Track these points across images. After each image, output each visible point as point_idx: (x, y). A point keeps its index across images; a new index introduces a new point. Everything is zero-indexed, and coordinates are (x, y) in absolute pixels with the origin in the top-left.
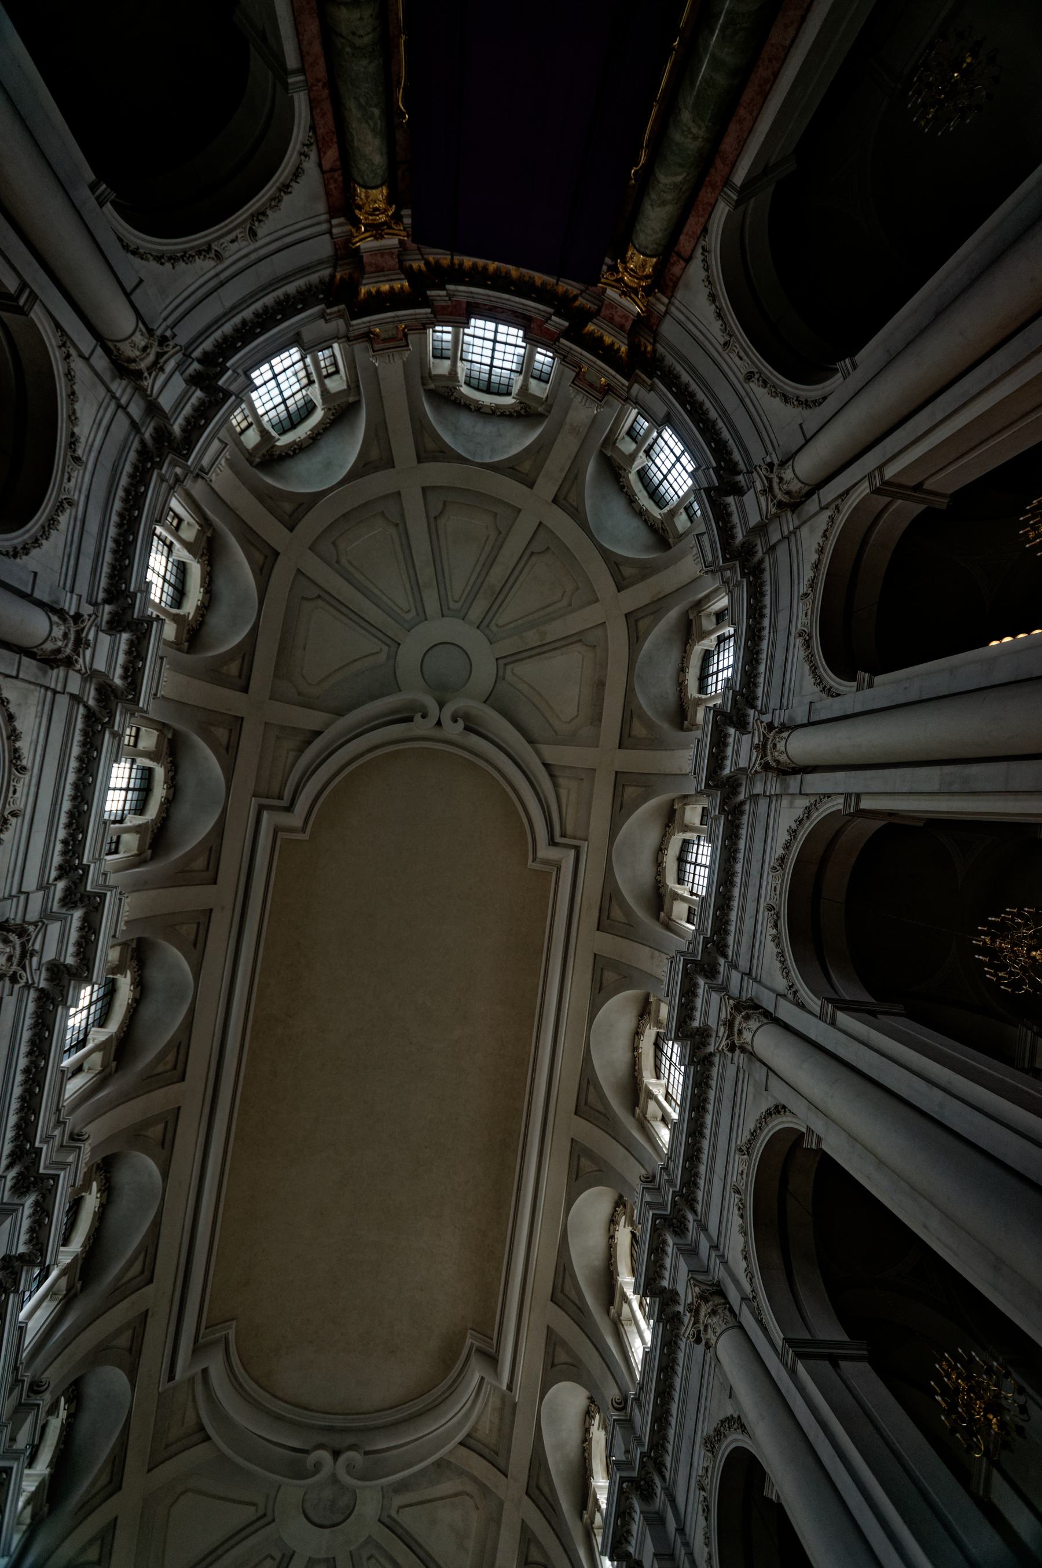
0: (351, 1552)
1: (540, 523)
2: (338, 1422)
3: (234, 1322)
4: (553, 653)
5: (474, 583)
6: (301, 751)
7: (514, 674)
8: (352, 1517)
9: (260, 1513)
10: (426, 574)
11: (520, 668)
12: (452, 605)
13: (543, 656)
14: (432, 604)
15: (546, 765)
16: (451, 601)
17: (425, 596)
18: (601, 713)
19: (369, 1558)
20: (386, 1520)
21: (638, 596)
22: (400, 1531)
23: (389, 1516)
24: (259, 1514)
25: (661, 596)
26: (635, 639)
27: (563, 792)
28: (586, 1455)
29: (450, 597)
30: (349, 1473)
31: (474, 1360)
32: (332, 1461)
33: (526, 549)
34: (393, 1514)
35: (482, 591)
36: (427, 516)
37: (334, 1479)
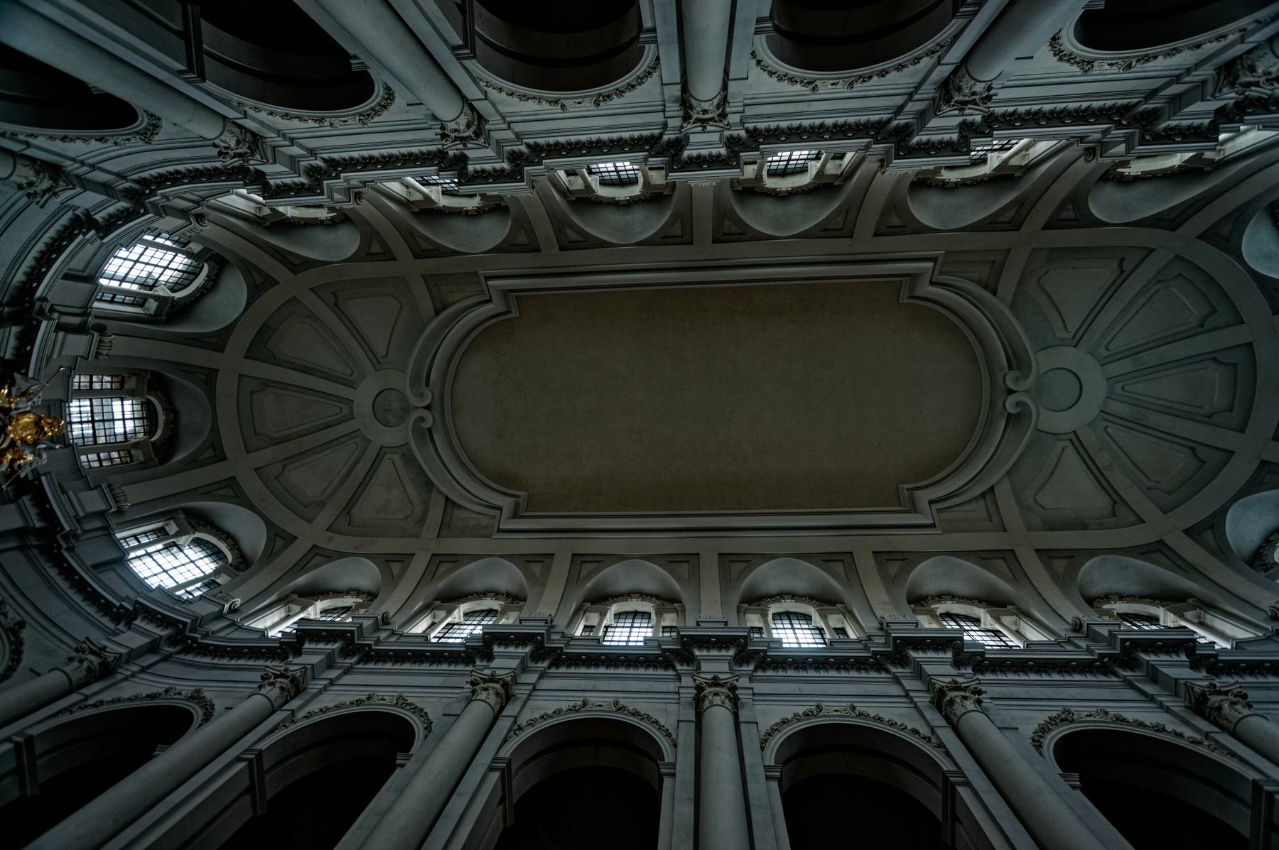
0: (359, 430)
1: (1233, 453)
2: (447, 406)
3: (518, 315)
4: (1094, 481)
5: (1148, 402)
6: (979, 283)
7: (1063, 449)
9: (381, 360)
10: (1148, 358)
11: (1070, 453)
12: (1118, 387)
13: (1088, 472)
14: (1115, 369)
15: (992, 489)
16: (1122, 384)
17: (1126, 360)
18: (1057, 530)
19: (356, 443)
21: (1191, 551)
22: (377, 463)
23: (385, 453)
24: (379, 359)
25: (1203, 571)
26: (1142, 552)
27: (973, 506)
28: (470, 597)
29: (1126, 382)
30: (416, 420)
31: (511, 500)
32: (423, 405)
33: (1196, 442)
34: (387, 456)
35: (1141, 409)
36: (1215, 351)
37: (407, 409)
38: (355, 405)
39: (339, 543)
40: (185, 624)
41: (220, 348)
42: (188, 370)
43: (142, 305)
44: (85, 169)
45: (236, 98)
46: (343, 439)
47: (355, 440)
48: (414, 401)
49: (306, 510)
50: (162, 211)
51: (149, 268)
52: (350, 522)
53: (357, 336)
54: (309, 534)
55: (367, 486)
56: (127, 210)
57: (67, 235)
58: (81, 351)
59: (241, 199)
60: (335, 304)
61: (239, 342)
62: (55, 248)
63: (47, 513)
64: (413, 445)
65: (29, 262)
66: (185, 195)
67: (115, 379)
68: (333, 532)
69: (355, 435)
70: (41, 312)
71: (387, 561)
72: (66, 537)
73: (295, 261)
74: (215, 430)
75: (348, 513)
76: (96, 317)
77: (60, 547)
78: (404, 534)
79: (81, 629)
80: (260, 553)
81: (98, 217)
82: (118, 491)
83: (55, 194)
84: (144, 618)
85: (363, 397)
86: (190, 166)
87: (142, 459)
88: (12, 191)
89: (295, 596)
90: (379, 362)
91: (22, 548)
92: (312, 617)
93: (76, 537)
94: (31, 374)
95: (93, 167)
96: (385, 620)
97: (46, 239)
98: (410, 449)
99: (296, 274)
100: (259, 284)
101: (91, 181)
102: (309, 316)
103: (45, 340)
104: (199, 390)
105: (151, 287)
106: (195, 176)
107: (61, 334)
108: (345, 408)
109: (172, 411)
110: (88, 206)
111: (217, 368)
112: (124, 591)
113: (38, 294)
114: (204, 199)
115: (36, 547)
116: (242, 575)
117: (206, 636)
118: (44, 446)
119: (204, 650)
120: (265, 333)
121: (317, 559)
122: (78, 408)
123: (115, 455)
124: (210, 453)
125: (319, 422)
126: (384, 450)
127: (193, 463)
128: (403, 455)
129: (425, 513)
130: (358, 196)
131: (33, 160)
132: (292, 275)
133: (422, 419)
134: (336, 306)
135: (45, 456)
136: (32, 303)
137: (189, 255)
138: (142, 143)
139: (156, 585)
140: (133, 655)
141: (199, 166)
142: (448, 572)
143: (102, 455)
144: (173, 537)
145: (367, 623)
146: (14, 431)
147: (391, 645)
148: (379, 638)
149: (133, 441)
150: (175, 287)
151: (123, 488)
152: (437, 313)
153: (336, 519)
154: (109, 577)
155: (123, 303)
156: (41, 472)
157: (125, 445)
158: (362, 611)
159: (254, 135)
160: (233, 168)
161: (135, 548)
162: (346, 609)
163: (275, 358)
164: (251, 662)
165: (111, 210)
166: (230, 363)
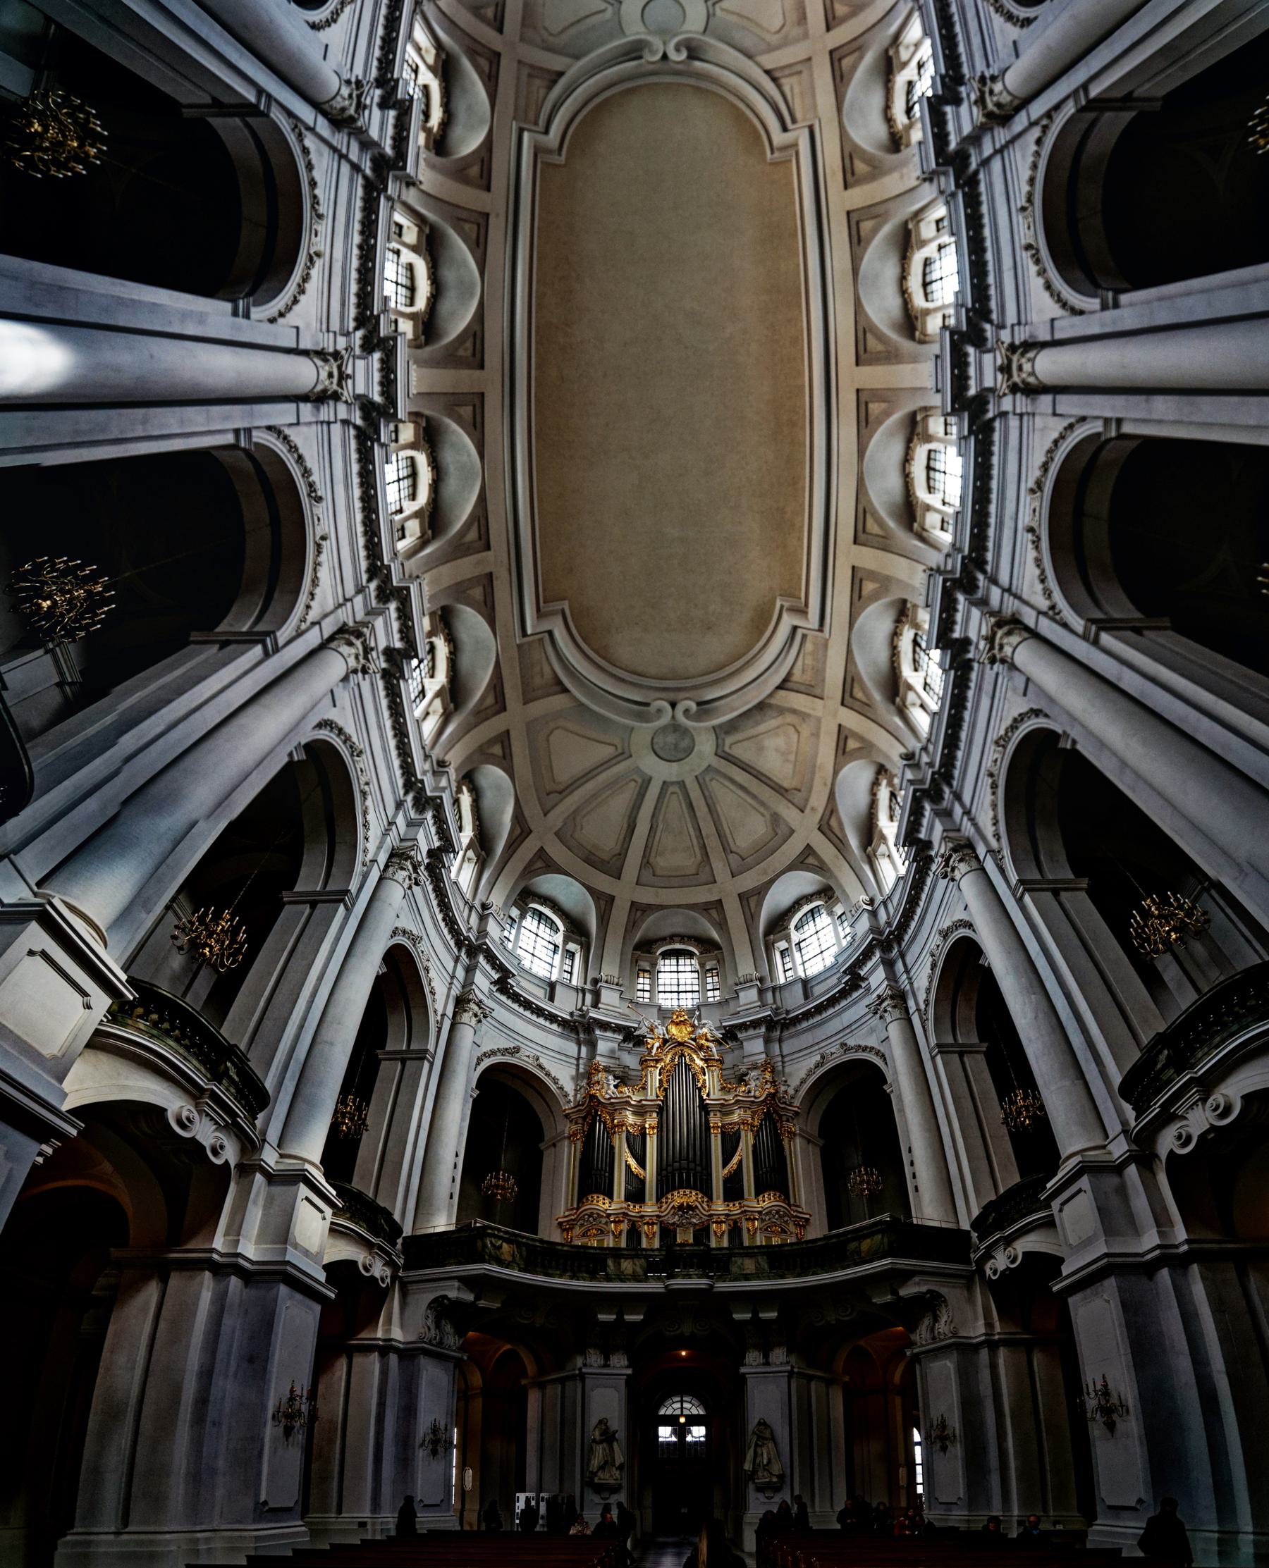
8: (693, 754)
9: (620, 751)
20: (723, 754)
22: (733, 760)
23: (724, 751)
34: (727, 749)
37: (675, 727)
38: (668, 780)
39: (818, 801)
40: (873, 939)
41: (611, 899)
42: (632, 925)
43: (572, 955)
44: (455, 981)
45: (358, 868)
46: (707, 794)
47: (707, 779)
48: (666, 719)
49: (779, 832)
50: (483, 933)
51: (538, 946)
52: (796, 789)
53: (595, 772)
54: (805, 830)
55: (759, 772)
56: (486, 957)
57: (516, 997)
58: (617, 995)
59: (461, 872)
60: (560, 793)
61: (604, 883)
62: (527, 1005)
63: (755, 1024)
64: (716, 722)
65: (541, 1021)
66: (466, 918)
67: (641, 975)
68: (805, 806)
69: (701, 781)
70: (583, 1016)
71: (844, 752)
72: (777, 1014)
73: (518, 831)
74: (692, 907)
75: (786, 790)
76: (585, 983)
77: (784, 1019)
78: (816, 735)
79: (860, 1009)
80: (816, 876)
81: (496, 976)
82: (742, 980)
83: (481, 1001)
84: (860, 968)
85: (661, 771)
86: (437, 910)
87: (714, 962)
88: (484, 1027)
89: (869, 849)
90: (623, 753)
91: (780, 1041)
92: (895, 830)
93: (777, 1009)
94: (636, 1026)
95: (453, 977)
96: (909, 757)
97: (521, 1010)
98: (720, 726)
99: (531, 831)
100: (544, 863)
101: (465, 982)
102: (574, 819)
103: (607, 1015)
104: (652, 917)
105: (556, 946)
106: (445, 906)
107: (600, 1005)
108: (672, 789)
109: (672, 938)
110: (488, 983)
111: (629, 904)
112: (834, 980)
113: (568, 1017)
114: (467, 902)
115: (781, 1032)
116: (838, 893)
117: (889, 924)
118: (696, 1023)
119: (903, 925)
120: (592, 860)
121: (833, 823)
122: (667, 1001)
123: (709, 980)
124: (714, 913)
125: (687, 816)
126: (720, 752)
127: (722, 925)
128: (727, 733)
129: (794, 711)
130: (442, 764)
131: (455, 1014)
132: (532, 835)
133: (686, 712)
134: (564, 791)
135: (703, 1022)
136: (575, 1022)
137: (523, 917)
138: (423, 942)
139: (833, 960)
140: (891, 977)
141: (435, 903)
142: (864, 689)
143: (709, 987)
144: (790, 945)
145: (909, 775)
146: (682, 1037)
147: (938, 751)
148: (927, 764)
149: (698, 967)
150: (553, 927)
151: (740, 975)
152: (566, 690)
153: (793, 804)
154: (818, 990)
155: (572, 966)
156: (718, 1025)
157: (703, 973)
158: (896, 781)
159: (392, 855)
160: (430, 876)
161: (796, 972)
162: (893, 795)
163: (620, 854)
164: (926, 889)
165: (488, 968)
166: (625, 891)
